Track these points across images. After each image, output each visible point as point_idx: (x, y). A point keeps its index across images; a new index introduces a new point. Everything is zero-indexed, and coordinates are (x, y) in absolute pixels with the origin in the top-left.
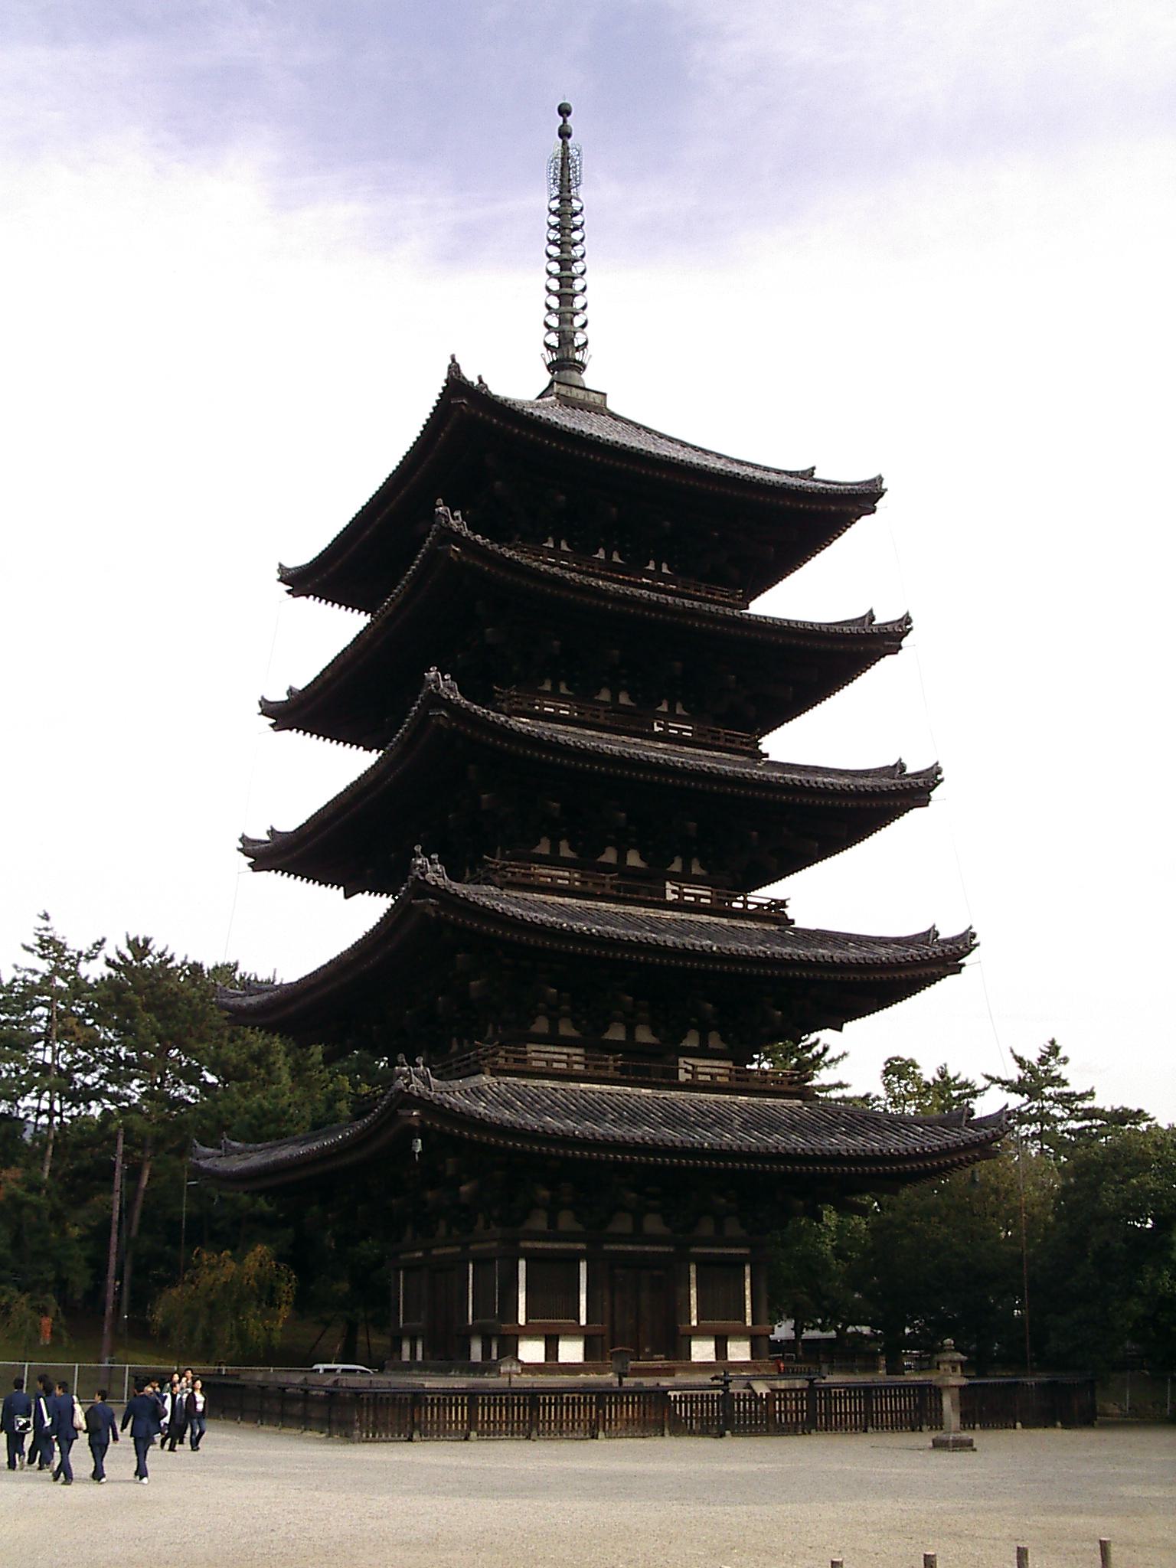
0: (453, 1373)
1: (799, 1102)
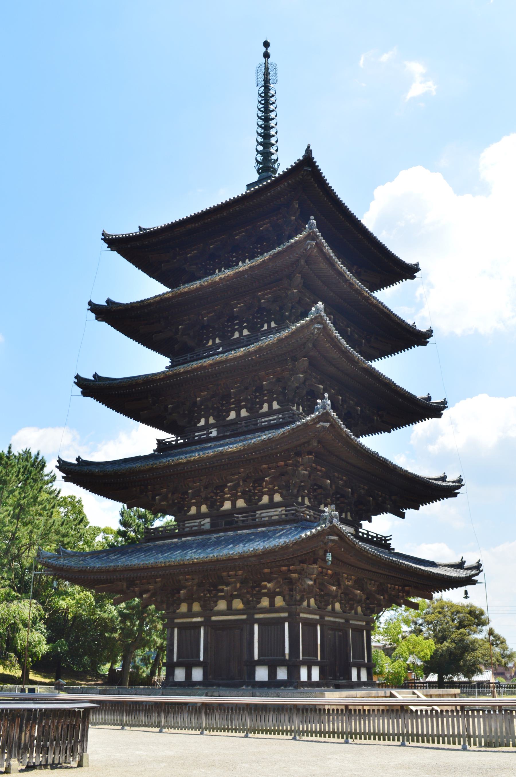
0: (244, 687)
1: (387, 551)
